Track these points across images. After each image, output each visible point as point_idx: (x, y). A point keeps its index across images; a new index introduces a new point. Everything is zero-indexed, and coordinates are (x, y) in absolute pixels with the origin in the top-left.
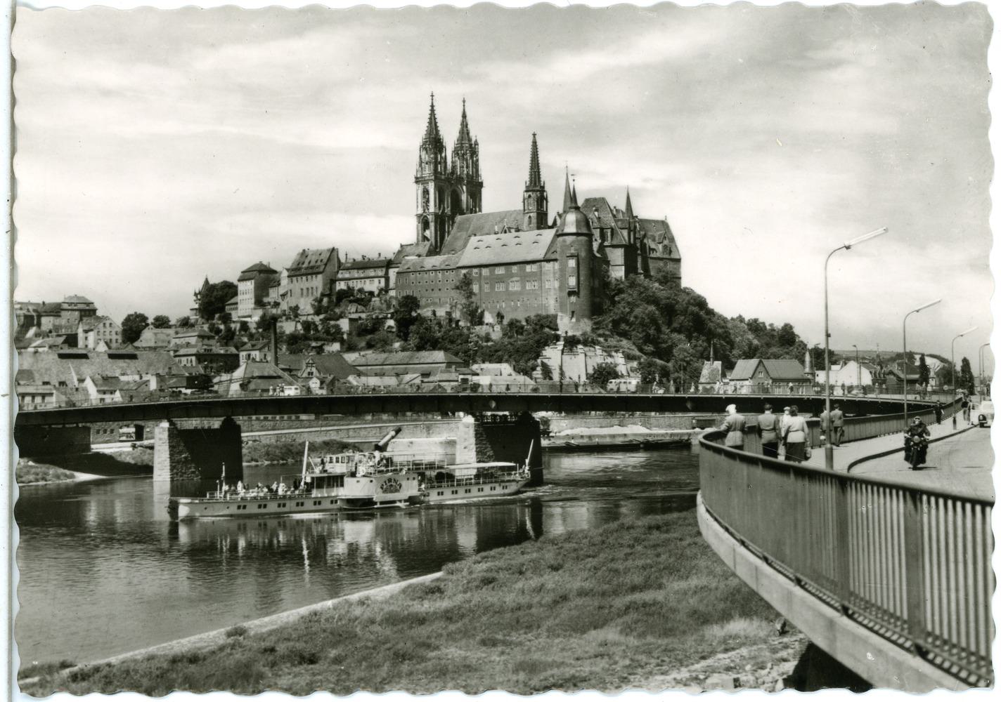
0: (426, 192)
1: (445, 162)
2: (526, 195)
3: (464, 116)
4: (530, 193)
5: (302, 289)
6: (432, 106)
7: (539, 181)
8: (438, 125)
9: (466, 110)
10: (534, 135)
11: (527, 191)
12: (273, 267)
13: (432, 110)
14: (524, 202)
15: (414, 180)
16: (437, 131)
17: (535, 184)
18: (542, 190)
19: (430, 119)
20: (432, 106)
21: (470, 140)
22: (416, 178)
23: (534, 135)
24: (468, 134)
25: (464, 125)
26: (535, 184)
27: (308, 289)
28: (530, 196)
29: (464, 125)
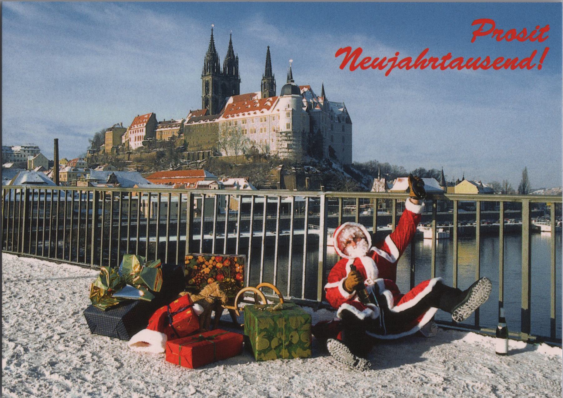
0: (207, 84)
1: (219, 67)
2: (263, 82)
3: (231, 43)
4: (266, 81)
5: (136, 137)
6: (212, 36)
7: (271, 74)
8: (215, 44)
9: (232, 40)
10: (268, 47)
11: (263, 80)
12: (124, 126)
13: (212, 38)
14: (262, 86)
15: (201, 77)
16: (215, 50)
17: (268, 75)
18: (273, 79)
19: (211, 43)
20: (212, 36)
21: (234, 56)
22: (202, 76)
23: (268, 47)
24: (233, 52)
25: (231, 47)
26: (268, 75)
27: (138, 137)
28: (265, 83)
29: (231, 47)
